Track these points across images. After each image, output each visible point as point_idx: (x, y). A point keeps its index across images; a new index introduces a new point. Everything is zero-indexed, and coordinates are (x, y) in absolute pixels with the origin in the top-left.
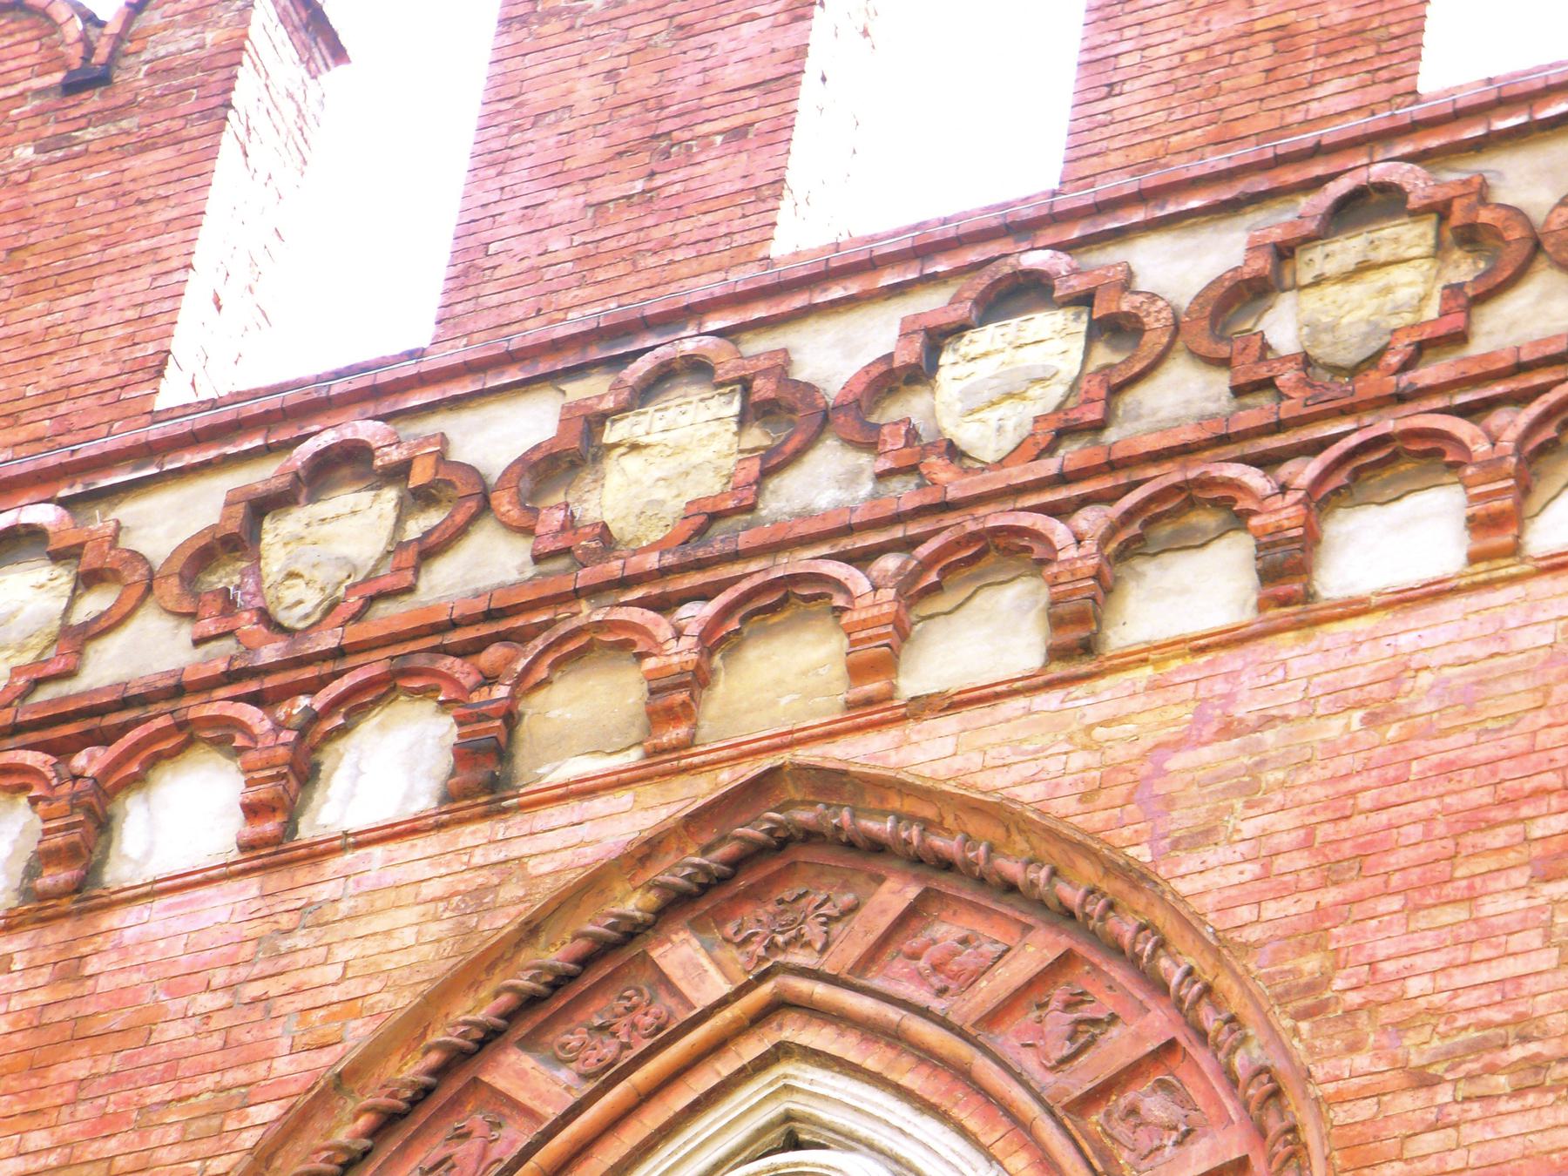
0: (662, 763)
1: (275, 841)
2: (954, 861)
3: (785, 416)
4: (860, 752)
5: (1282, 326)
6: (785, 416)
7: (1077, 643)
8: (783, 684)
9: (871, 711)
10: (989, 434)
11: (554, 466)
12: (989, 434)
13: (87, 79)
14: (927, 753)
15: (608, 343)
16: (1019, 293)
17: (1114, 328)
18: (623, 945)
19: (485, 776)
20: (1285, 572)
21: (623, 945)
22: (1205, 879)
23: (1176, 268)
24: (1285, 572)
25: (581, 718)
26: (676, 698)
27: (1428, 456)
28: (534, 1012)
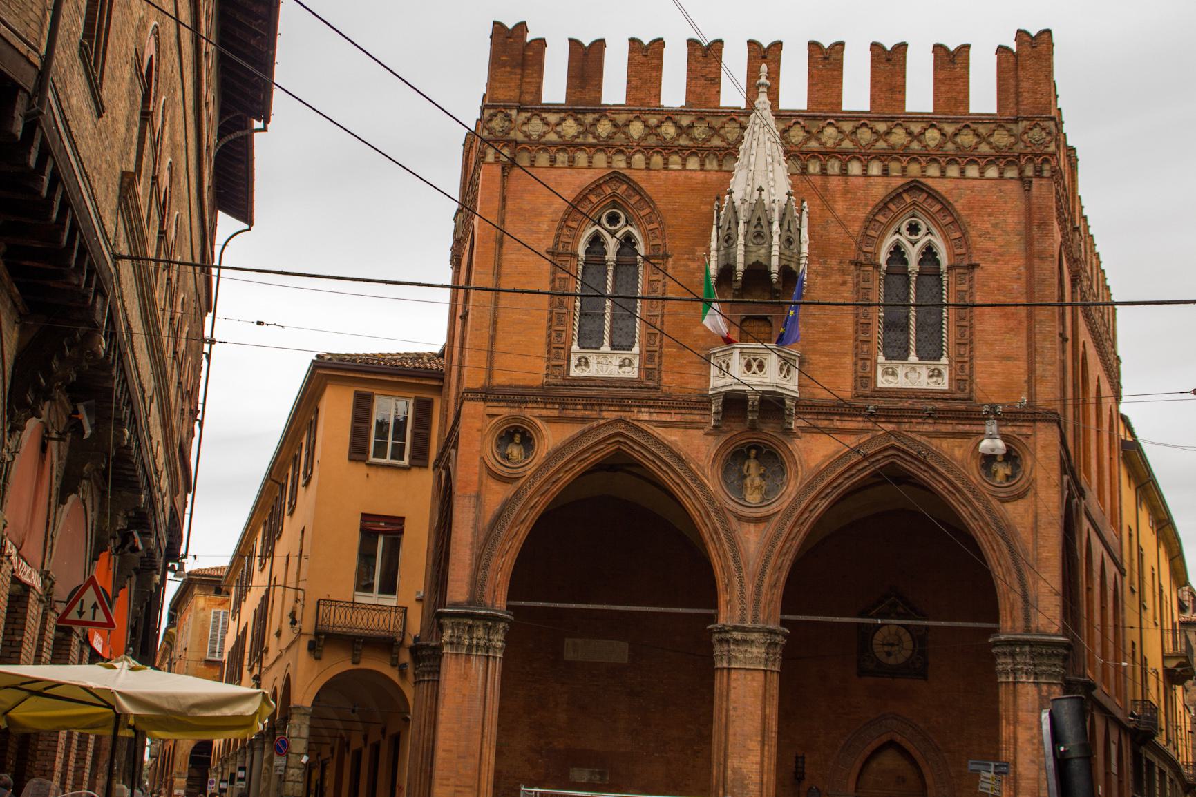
0: (904, 176)
1: (865, 174)
2: (933, 195)
3: (910, 133)
4: (922, 180)
5: (958, 139)
6: (910, 133)
7: (943, 174)
8: (914, 169)
9: (924, 176)
10: (932, 144)
11: (888, 133)
12: (932, 144)
13: (826, 58)
14: (929, 182)
15: (892, 119)
16: (932, 126)
17: (943, 135)
18: (899, 195)
19: (886, 172)
20: (962, 172)
21: (899, 195)
22: (958, 206)
23: (949, 129)
24: (962, 172)
25: (894, 167)
26: (904, 169)
27: (975, 162)
28: (892, 200)
